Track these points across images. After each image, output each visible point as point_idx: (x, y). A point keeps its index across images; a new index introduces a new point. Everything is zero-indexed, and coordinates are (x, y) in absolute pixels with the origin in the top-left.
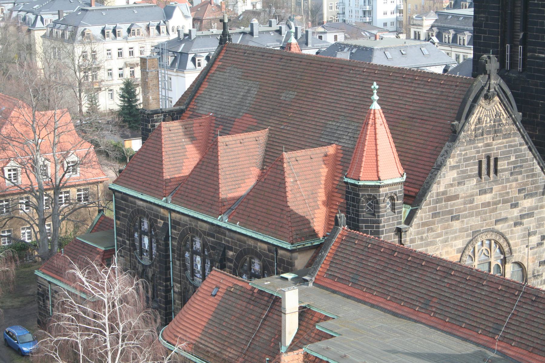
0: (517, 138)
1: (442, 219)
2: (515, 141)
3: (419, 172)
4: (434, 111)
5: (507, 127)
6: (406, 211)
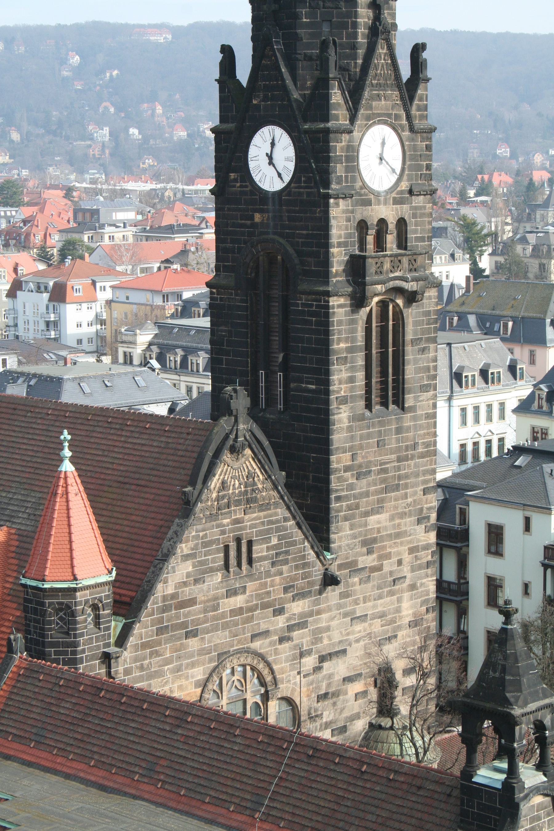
0: (279, 510)
1: (171, 636)
2: (276, 514)
3: (135, 565)
4: (155, 473)
5: (264, 494)
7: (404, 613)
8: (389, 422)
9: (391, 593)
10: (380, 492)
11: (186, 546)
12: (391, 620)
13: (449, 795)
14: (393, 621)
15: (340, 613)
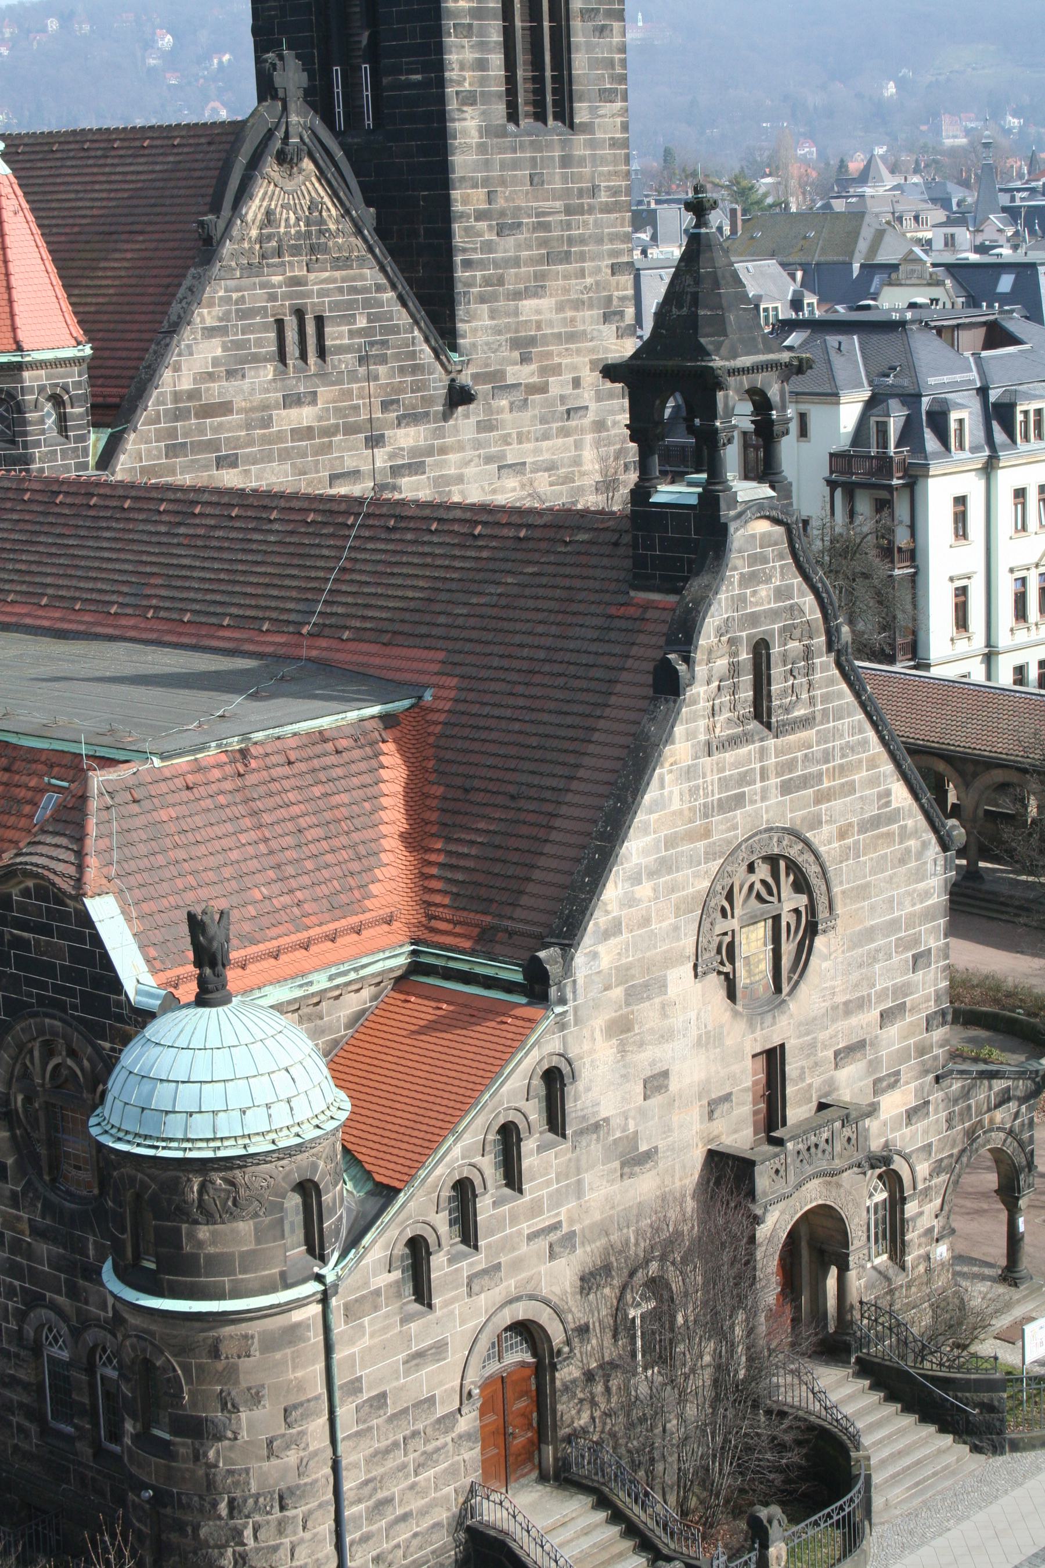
0: (367, 272)
1: (192, 461)
2: (363, 278)
3: (127, 349)
4: (158, 210)
5: (340, 241)
6: (96, 440)
7: (587, 467)
8: (549, 146)
9: (565, 432)
10: (539, 261)
11: (209, 313)
12: (566, 477)
13: (616, 544)
14: (568, 479)
15: (479, 456)
